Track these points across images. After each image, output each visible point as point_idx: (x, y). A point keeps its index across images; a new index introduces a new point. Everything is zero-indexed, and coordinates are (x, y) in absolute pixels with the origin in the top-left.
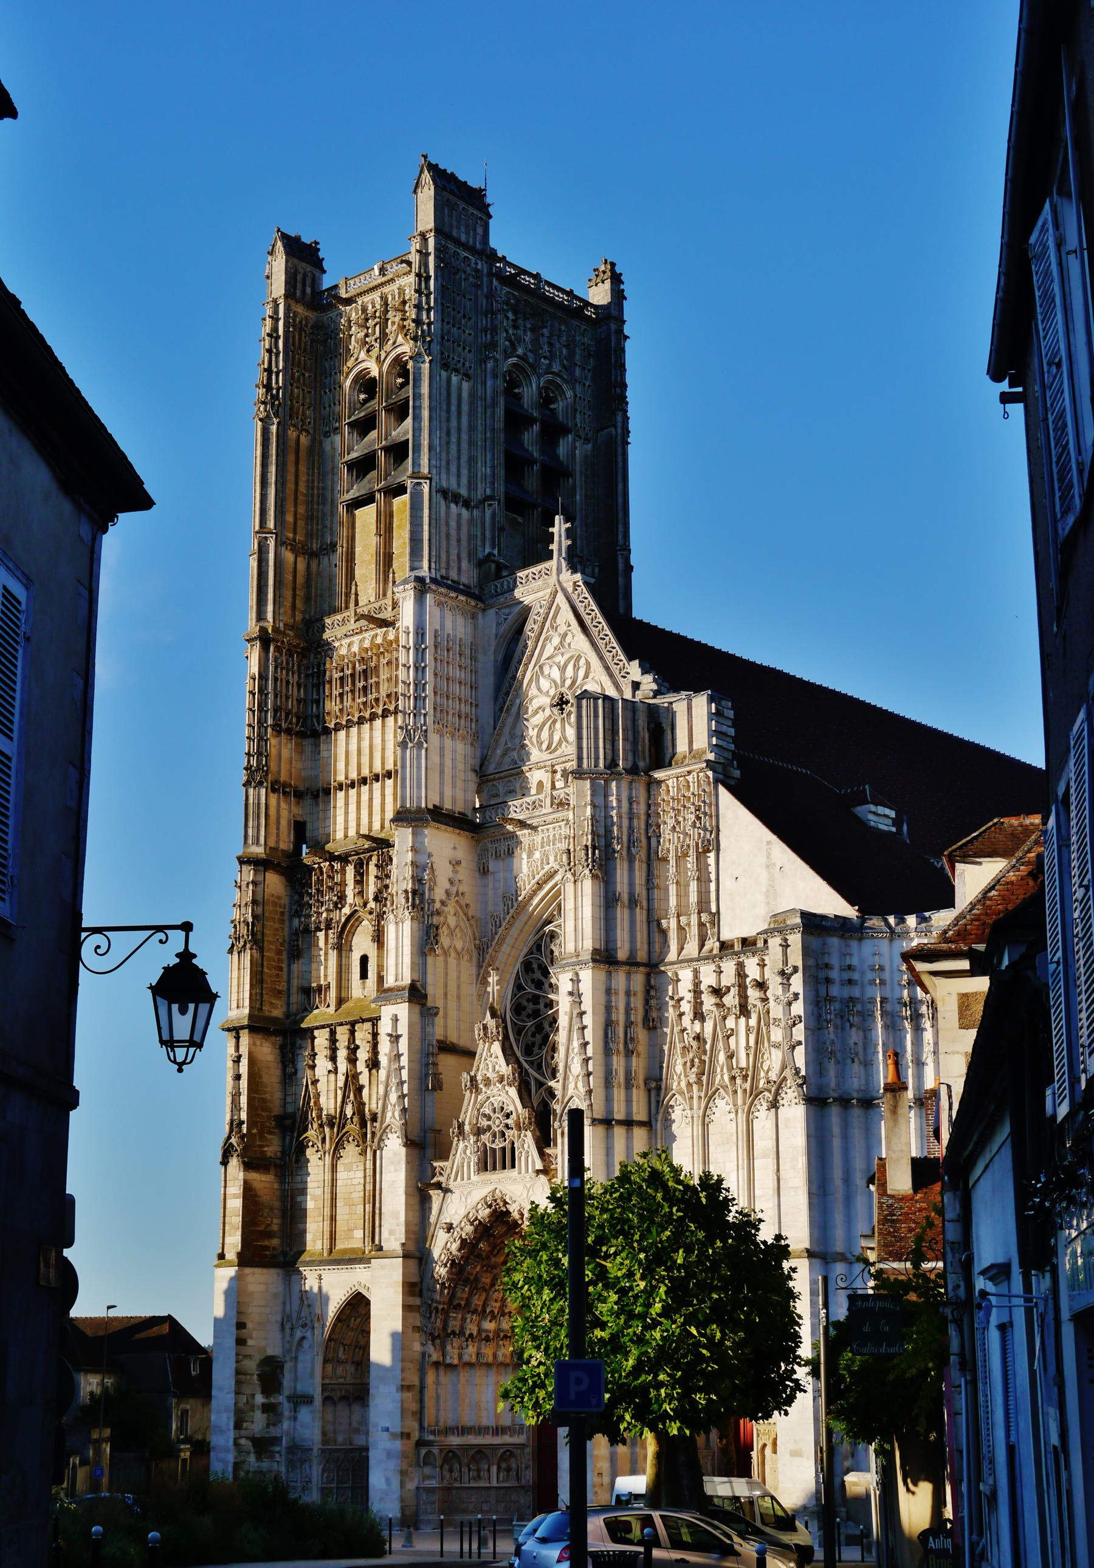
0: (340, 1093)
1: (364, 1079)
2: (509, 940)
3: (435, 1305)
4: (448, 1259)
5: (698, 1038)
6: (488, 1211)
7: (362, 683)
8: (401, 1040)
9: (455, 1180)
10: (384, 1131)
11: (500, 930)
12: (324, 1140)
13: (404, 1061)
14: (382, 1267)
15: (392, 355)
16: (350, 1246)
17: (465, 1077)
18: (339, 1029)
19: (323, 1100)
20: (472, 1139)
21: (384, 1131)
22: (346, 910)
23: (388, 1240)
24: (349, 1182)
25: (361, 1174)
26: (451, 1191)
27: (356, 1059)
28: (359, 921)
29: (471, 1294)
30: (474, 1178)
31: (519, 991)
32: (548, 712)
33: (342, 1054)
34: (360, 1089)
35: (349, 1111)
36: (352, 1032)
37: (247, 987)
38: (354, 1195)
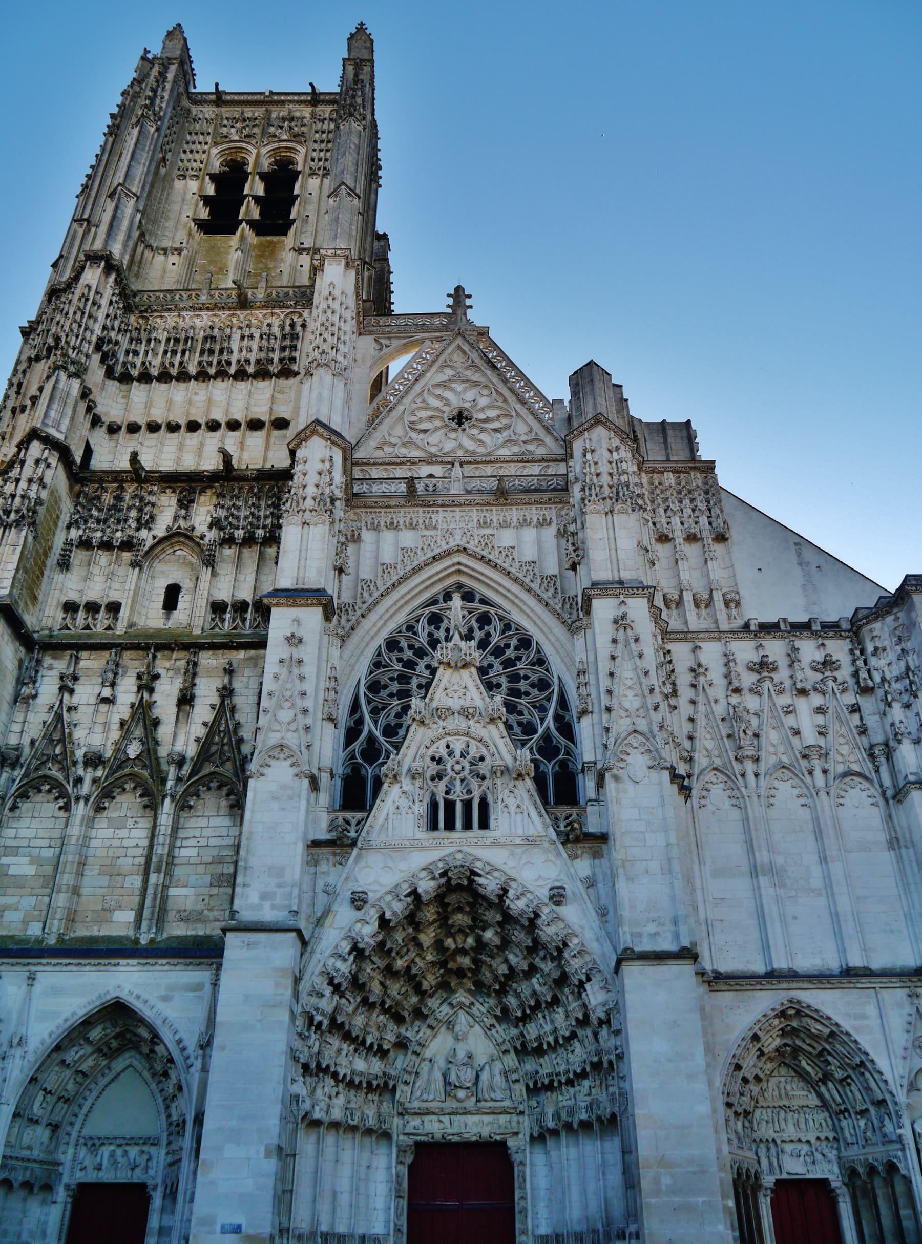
0: (115, 726)
3: (318, 1018)
6: (433, 884)
7: (208, 346)
12: (79, 780)
15: (275, 145)
16: (102, 933)
19: (79, 734)
22: (160, 530)
23: (259, 907)
24: (116, 843)
29: (356, 1009)
31: (378, 668)
32: (438, 423)
34: (156, 723)
35: (133, 750)
36: (154, 657)
37: (13, 566)
38: (119, 862)
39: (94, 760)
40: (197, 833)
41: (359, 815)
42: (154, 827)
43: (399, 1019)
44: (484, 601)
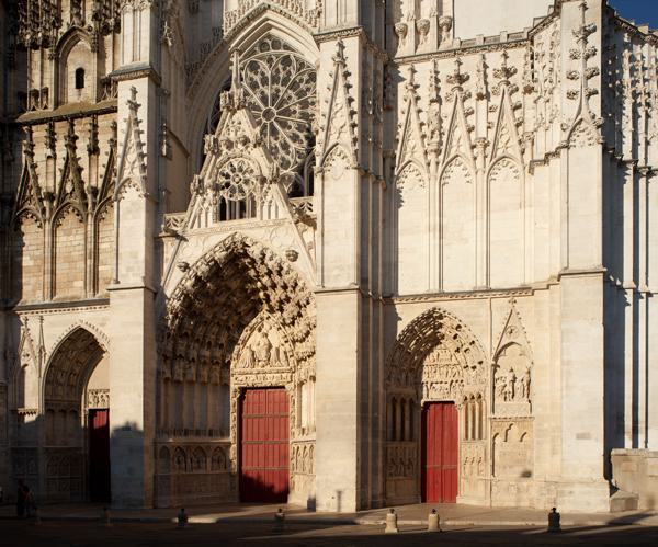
1: (84, 162)
2: (214, 65)
4: (183, 293)
5: (438, 114)
6: (224, 253)
8: (139, 109)
9: (192, 227)
10: (123, 185)
11: (210, 55)
13: (144, 126)
14: (122, 297)
17: (209, 138)
18: (57, 124)
19: (41, 181)
20: (210, 192)
21: (123, 185)
22: (64, 29)
24: (69, 244)
25: (78, 239)
26: (186, 240)
27: (75, 148)
28: (76, 40)
30: (216, 225)
33: (61, 145)
34: (80, 170)
35: (69, 188)
36: (72, 125)
39: (50, 197)
40: (108, 233)
41: (182, 215)
42: (86, 232)
43: (229, 329)
44: (287, 47)
